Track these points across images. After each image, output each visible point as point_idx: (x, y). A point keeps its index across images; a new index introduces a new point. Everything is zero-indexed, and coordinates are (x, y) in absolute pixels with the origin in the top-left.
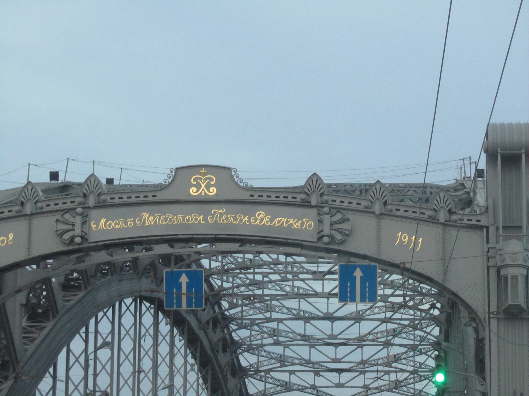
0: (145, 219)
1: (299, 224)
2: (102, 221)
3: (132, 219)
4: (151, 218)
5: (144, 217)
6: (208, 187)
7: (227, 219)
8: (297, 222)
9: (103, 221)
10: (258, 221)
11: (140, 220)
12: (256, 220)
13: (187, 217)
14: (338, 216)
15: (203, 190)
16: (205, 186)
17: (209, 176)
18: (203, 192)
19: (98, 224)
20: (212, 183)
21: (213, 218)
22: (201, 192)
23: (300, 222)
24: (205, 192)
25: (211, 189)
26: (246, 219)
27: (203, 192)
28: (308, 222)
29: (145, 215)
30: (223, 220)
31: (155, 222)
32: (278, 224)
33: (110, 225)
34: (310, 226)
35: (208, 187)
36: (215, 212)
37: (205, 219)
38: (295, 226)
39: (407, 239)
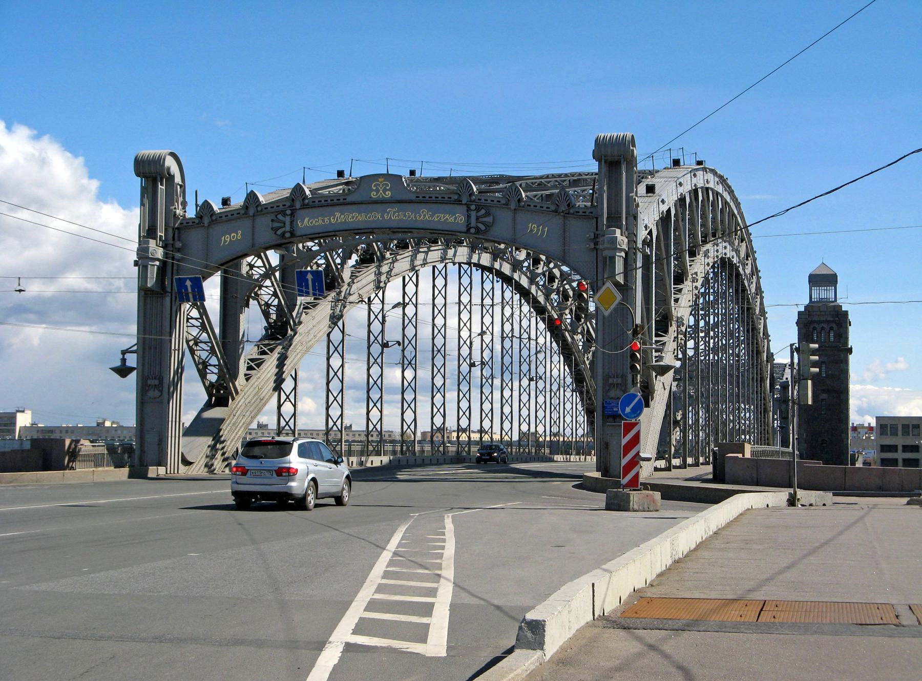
1: (452, 219)
2: (306, 219)
4: (342, 216)
6: (385, 191)
7: (398, 215)
9: (306, 220)
10: (422, 217)
13: (369, 216)
14: (483, 212)
19: (302, 222)
20: (388, 188)
21: (388, 215)
25: (387, 193)
28: (460, 217)
29: (338, 214)
33: (311, 223)
35: (385, 191)
36: (390, 211)
37: (382, 216)
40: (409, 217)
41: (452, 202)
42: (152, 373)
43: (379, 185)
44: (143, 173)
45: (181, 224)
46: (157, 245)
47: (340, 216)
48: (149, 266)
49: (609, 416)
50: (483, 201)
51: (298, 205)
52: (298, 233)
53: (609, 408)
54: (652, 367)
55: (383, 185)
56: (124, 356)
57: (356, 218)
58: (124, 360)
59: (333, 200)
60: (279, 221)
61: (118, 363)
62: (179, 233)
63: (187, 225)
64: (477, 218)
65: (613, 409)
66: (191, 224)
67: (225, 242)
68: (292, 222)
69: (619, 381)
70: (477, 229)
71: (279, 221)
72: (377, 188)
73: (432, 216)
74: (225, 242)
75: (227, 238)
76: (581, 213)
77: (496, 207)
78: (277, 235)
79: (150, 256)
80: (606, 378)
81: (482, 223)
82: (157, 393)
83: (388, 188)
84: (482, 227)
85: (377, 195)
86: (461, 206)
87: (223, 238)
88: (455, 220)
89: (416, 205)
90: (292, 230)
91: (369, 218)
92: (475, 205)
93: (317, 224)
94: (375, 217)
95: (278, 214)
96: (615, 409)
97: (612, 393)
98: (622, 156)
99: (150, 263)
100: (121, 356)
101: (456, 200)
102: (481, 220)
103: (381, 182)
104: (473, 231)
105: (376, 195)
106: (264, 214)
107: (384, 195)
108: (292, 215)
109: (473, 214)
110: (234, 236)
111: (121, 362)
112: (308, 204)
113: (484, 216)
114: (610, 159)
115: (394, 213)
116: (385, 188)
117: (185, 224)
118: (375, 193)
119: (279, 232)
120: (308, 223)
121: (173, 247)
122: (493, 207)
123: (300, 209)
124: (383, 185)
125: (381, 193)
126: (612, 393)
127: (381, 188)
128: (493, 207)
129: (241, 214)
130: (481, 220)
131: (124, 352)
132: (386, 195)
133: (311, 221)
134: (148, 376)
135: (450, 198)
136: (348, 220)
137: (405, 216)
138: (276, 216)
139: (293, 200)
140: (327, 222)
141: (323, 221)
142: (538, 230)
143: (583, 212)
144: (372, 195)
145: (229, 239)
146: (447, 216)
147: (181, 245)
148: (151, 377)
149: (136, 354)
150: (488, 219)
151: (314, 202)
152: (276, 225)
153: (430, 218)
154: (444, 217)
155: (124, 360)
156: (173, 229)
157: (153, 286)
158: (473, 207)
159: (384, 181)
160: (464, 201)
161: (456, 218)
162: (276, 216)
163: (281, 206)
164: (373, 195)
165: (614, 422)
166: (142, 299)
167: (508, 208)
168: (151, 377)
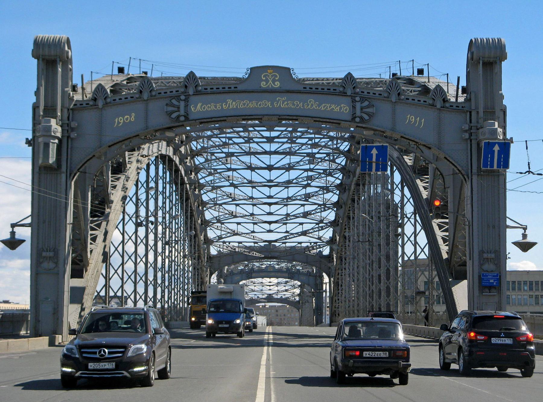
0: (229, 104)
1: (338, 108)
3: (220, 104)
4: (234, 103)
5: (228, 103)
6: (274, 81)
7: (287, 104)
8: (337, 107)
9: (199, 105)
12: (308, 105)
13: (260, 103)
14: (366, 103)
19: (196, 107)
20: (276, 79)
22: (269, 85)
24: (271, 85)
25: (276, 83)
26: (301, 105)
28: (344, 107)
29: (230, 101)
31: (237, 106)
33: (204, 108)
34: (346, 110)
35: (274, 81)
36: (279, 100)
37: (272, 104)
38: (336, 110)
39: (413, 119)
40: (298, 105)
41: (337, 94)
42: (46, 246)
43: (269, 76)
44: (42, 56)
45: (75, 105)
46: (57, 124)
47: (232, 103)
48: (51, 144)
49: (485, 287)
50: (366, 93)
51: (191, 91)
52: (191, 117)
53: (486, 280)
54: (519, 244)
55: (272, 76)
56: (13, 230)
57: (248, 105)
58: (13, 233)
59: (224, 88)
60: (173, 105)
61: (7, 236)
62: (73, 112)
63: (81, 106)
64: (362, 109)
65: (489, 281)
66: (84, 105)
67: (119, 123)
68: (186, 106)
69: (493, 256)
70: (361, 118)
71: (173, 105)
72: (266, 78)
73: (319, 106)
74: (119, 123)
75: (121, 120)
76: (454, 107)
77: (377, 99)
78: (172, 118)
79: (53, 134)
80: (481, 252)
81: (366, 114)
82: (51, 265)
83: (276, 79)
84: (366, 117)
85: (266, 84)
86: (344, 98)
89: (305, 96)
90: (186, 114)
91: (260, 105)
93: (209, 109)
94: (266, 105)
95: (172, 99)
96: (491, 281)
97: (486, 267)
98: (498, 58)
99: (52, 141)
100: (10, 230)
101: (340, 92)
102: (364, 110)
103: (271, 73)
104: (357, 120)
105: (265, 85)
106: (156, 99)
108: (186, 100)
109: (358, 105)
110: (128, 118)
111: (11, 235)
112: (201, 90)
113: (368, 107)
114: (486, 60)
116: (274, 78)
117: (78, 105)
118: (265, 83)
119: (174, 115)
120: (201, 109)
121: (68, 126)
122: (374, 99)
123: (193, 95)
124: (272, 76)
125: (270, 83)
126: (486, 267)
127: (270, 79)
128: (374, 99)
129: (135, 98)
130: (364, 110)
131: (13, 226)
132: (275, 85)
133: (203, 106)
134: (42, 248)
135: (335, 90)
136: (239, 106)
137: (294, 105)
138: (170, 101)
139: (186, 87)
141: (216, 107)
142: (416, 121)
143: (457, 106)
144: (262, 85)
145: (122, 121)
146: (333, 106)
147: (77, 125)
148: (45, 250)
149: (30, 228)
151: (206, 89)
152: (170, 109)
153: (317, 107)
154: (330, 107)
155: (13, 233)
156: (68, 110)
157: (53, 163)
158: (358, 99)
159: (273, 73)
160: (349, 93)
161: (341, 108)
162: (170, 101)
163: (174, 92)
164: (263, 85)
165: (490, 293)
166: (36, 176)
167: (388, 101)
168: (45, 250)
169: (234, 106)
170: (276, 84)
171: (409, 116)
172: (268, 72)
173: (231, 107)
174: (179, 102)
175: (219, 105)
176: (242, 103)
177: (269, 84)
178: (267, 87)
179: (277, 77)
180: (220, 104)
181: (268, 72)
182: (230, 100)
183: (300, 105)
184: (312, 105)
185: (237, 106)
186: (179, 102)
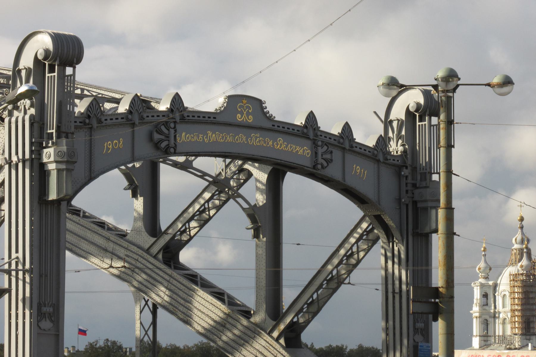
0: (210, 136)
1: (301, 151)
2: (183, 134)
3: (202, 135)
4: (214, 135)
5: (209, 135)
6: (248, 114)
7: (260, 141)
8: (301, 149)
10: (279, 146)
11: (207, 138)
12: (278, 144)
13: (236, 138)
14: (325, 148)
15: (245, 116)
16: (246, 114)
17: (250, 105)
18: (245, 118)
19: (181, 137)
20: (250, 111)
21: (251, 140)
22: (244, 119)
23: (302, 149)
24: (246, 119)
25: (250, 117)
26: (271, 143)
27: (245, 118)
28: (307, 150)
29: (210, 133)
30: (257, 142)
31: (217, 139)
32: (290, 149)
33: (188, 138)
34: (308, 154)
35: (248, 114)
36: (253, 136)
37: (247, 140)
38: (300, 153)
39: (359, 170)
40: (268, 144)
57: (226, 138)
67: (108, 149)
73: (286, 147)
74: (108, 149)
84: (325, 164)
87: (106, 145)
88: (303, 153)
91: (237, 140)
92: (322, 142)
102: (324, 156)
103: (245, 104)
105: (239, 118)
107: (248, 120)
109: (320, 151)
110: (116, 143)
115: (256, 138)
133: (187, 136)
137: (265, 142)
140: (201, 140)
142: (361, 171)
145: (111, 146)
150: (328, 156)
158: (320, 143)
161: (304, 151)
169: (214, 140)
170: (250, 119)
171: (355, 166)
172: (242, 102)
173: (212, 140)
174: (169, 130)
175: (201, 136)
176: (221, 136)
177: (243, 117)
178: (242, 121)
179: (250, 110)
180: (202, 135)
181: (242, 102)
182: (209, 132)
183: (270, 143)
184: (281, 145)
185: (217, 139)
186: (169, 130)
